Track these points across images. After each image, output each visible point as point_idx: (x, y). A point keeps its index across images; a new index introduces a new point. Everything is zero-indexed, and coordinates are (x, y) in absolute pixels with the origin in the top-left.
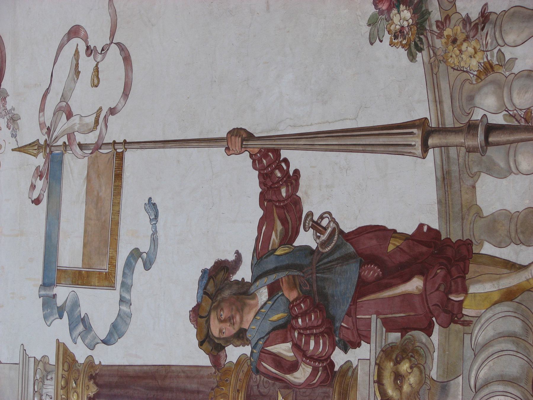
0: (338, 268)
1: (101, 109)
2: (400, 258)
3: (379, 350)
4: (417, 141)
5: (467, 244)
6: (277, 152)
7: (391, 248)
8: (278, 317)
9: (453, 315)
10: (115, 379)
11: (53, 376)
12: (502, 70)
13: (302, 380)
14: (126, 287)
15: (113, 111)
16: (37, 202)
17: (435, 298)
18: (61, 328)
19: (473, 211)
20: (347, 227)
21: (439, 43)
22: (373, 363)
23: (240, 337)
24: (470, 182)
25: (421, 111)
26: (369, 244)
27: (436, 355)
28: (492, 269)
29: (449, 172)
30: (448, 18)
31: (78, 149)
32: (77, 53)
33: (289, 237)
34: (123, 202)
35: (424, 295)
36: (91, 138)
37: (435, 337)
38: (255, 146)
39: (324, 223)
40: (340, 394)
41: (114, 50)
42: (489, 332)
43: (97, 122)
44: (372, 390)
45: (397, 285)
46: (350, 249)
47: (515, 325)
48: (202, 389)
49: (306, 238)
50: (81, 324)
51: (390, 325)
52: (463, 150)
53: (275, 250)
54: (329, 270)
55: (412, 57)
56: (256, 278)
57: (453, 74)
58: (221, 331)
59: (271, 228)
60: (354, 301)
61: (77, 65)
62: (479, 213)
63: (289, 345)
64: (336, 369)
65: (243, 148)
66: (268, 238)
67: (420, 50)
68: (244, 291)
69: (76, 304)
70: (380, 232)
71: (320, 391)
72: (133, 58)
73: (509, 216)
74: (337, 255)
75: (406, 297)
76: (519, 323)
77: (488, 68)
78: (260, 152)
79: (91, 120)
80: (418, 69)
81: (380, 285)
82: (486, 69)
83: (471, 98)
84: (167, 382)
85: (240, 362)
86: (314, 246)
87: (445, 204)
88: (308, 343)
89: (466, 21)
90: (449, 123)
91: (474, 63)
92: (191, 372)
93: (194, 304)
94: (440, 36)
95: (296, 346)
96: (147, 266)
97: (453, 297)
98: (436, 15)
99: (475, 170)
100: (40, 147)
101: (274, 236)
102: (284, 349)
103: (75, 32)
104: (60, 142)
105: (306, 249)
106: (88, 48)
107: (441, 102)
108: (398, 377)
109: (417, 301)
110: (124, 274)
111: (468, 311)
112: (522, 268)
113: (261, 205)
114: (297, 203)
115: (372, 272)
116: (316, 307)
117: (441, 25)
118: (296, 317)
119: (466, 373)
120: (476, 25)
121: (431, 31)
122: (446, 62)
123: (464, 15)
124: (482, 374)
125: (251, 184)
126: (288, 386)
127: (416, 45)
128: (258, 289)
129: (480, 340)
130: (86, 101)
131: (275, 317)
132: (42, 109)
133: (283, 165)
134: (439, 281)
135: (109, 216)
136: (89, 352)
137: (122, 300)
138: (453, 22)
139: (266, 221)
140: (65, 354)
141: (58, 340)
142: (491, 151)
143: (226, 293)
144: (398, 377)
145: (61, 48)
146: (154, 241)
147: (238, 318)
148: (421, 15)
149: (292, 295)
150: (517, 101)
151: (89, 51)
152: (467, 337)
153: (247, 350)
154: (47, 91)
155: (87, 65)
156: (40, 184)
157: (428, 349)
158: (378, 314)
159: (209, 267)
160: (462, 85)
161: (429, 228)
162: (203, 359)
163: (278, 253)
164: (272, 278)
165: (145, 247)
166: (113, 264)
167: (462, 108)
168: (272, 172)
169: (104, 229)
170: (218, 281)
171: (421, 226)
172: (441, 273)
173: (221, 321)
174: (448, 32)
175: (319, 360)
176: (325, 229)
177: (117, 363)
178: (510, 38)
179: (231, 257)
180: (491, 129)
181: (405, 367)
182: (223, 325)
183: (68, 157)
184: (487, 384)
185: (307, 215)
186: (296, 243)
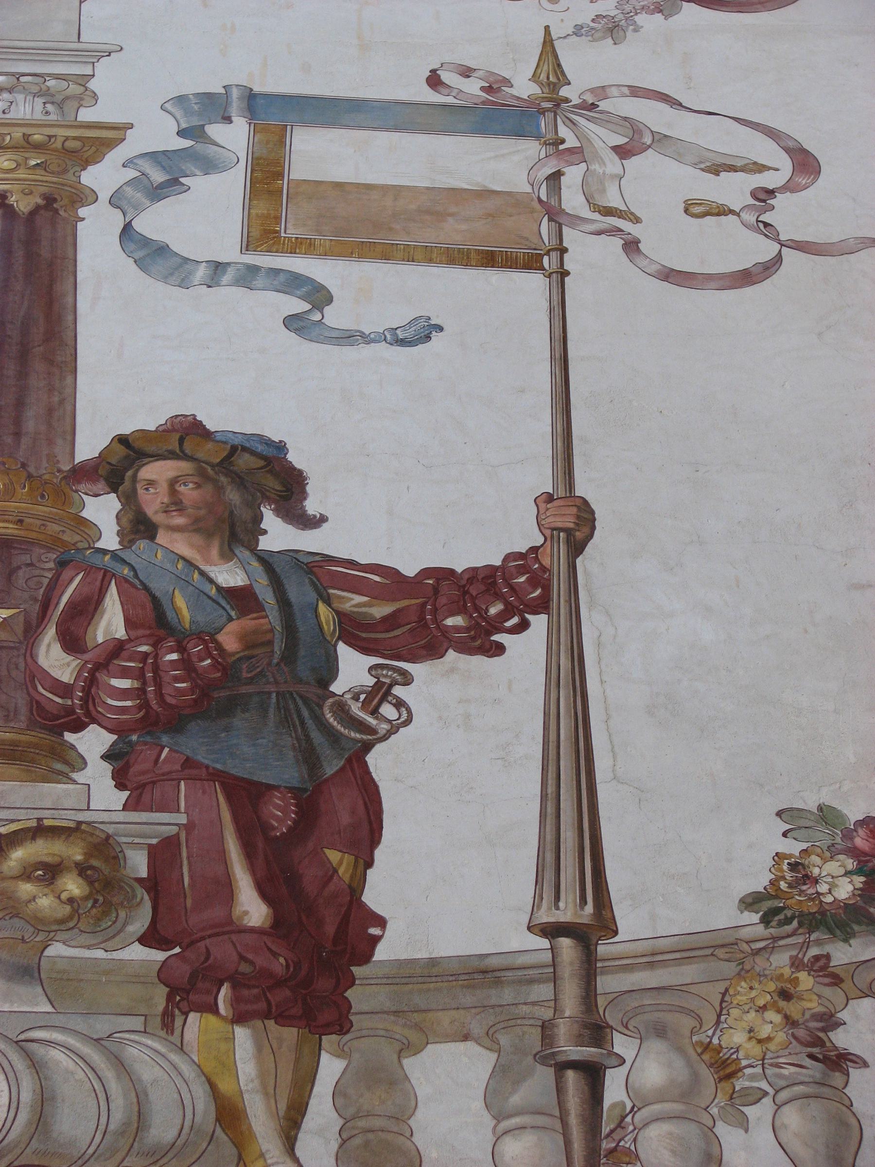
0: (288, 741)
1: (637, 220)
2: (310, 875)
3: (110, 829)
4: (566, 913)
6: (542, 606)
7: (333, 856)
8: (183, 609)
9: (184, 994)
10: (45, 252)
11: (53, 117)
12: (721, 1099)
13: (43, 661)
14: (248, 277)
15: (632, 246)
17: (223, 951)
18: (157, 132)
19: (414, 1036)
20: (378, 761)
21: (781, 960)
22: (81, 817)
23: (138, 526)
24: (477, 1029)
25: (632, 923)
26: (342, 808)
27: (99, 954)
28: (286, 1077)
29: (498, 982)
30: (836, 980)
31: (549, 171)
32: (759, 168)
33: (357, 633)
34: (435, 271)
35: (230, 927)
36: (572, 200)
37: (137, 953)
38: (556, 559)
40: (14, 743)
41: (767, 250)
43: (608, 212)
44: (21, 814)
46: (331, 767)
47: (163, 1129)
48: (25, 441)
49: (353, 669)
50: (167, 176)
51: (163, 853)
52: (548, 1014)
53: (328, 602)
55: (750, 902)
56: (266, 561)
57: (714, 993)
58: (151, 483)
59: (377, 594)
61: (733, 169)
62: (409, 1048)
63: (120, 632)
64: (69, 737)
65: (550, 532)
66: (355, 586)
67: (766, 920)
68: (238, 535)
69: (209, 166)
70: (366, 832)
71: (20, 700)
72: (748, 291)
73: (402, 1116)
74: (317, 737)
75: (225, 890)
76: (169, 1135)
77: (726, 1069)
78: (543, 569)
79: (613, 200)
80: (725, 915)
81: (251, 833)
82: (724, 1063)
83: (661, 1031)
84: (38, 366)
86: (338, 687)
87: (429, 973)
88: (124, 673)
89: (829, 1021)
90: (606, 984)
91: (738, 1038)
92: (61, 419)
93: (211, 426)
94: (796, 964)
95: (117, 648)
96: (293, 322)
97: (224, 992)
98: (842, 954)
99: (504, 1040)
100: (554, 87)
101: (359, 599)
102: (111, 622)
103: (806, 164)
104: (563, 131)
105: (330, 670)
106: (771, 193)
107: (651, 965)
108: (50, 872)
109: (216, 913)
110: (276, 272)
111: (195, 1024)
112: (290, 1143)
113: (427, 572)
114: (432, 650)
115: (279, 814)
116: (204, 691)
117: (821, 966)
118: (180, 648)
121: (807, 945)
123: (843, 1015)
124: (56, 1054)
126: (31, 631)
127: (776, 911)
129: (132, 1052)
130: (654, 187)
131: (181, 602)
132: (636, 92)
133: (515, 620)
134: (261, 961)
135: (402, 239)
136: (104, 196)
137: (218, 267)
138: (827, 992)
140: (100, 142)
141: (131, 126)
142: (545, 1075)
143: (233, 496)
144: (50, 872)
146: (349, 338)
147: (180, 521)
148: (841, 922)
150: (654, 1132)
152: (137, 1023)
153: (110, 541)
155: (734, 190)
156: (473, 87)
157: (109, 938)
158: (189, 827)
159: (290, 457)
160: (688, 1012)
161: (376, 939)
162: (89, 444)
163: (322, 608)
164: (266, 595)
165: (335, 317)
166: (297, 247)
167: (638, 1011)
168: (499, 596)
169: (373, 228)
170: (264, 476)
171: (381, 922)
172: (279, 965)
173: (173, 483)
174: (806, 980)
175: (88, 698)
176: (375, 712)
177: (80, 257)
178: (791, 1117)
179: (312, 506)
180: (593, 1075)
182: (163, 488)
183: (531, 148)
184: (36, 1065)
185: (404, 673)
186: (343, 649)
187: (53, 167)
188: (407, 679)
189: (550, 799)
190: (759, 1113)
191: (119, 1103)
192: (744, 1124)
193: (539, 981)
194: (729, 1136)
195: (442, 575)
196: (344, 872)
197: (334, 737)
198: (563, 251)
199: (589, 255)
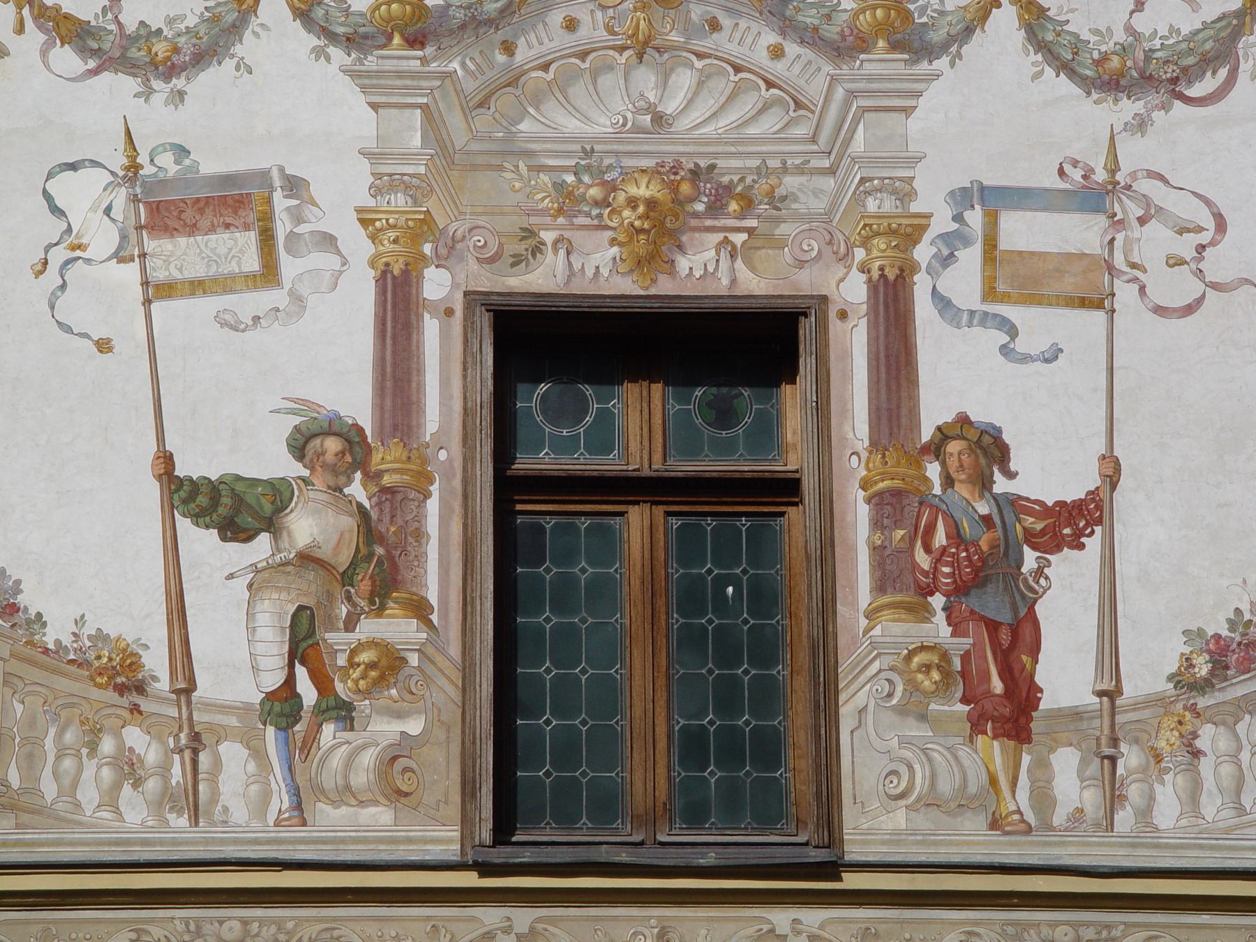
0: (1007, 599)
1: (1145, 271)
3: (946, 647)
4: (1105, 687)
5: (1028, 740)
6: (1099, 522)
7: (1024, 658)
9: (976, 725)
11: (899, 210)
12: (1156, 772)
13: (918, 559)
14: (986, 319)
15: (1142, 289)
16: (1061, 172)
17: (988, 706)
19: (1053, 744)
21: (1180, 706)
22: (937, 641)
23: (948, 482)
24: (1075, 742)
25: (1129, 690)
26: (1027, 631)
27: (946, 708)
28: (1011, 764)
29: (1081, 719)
30: (1198, 715)
32: (1199, 229)
33: (1031, 538)
34: (1060, 311)
35: (989, 693)
36: (1119, 261)
38: (1105, 494)
39: (1042, 581)
40: (910, 603)
42: (966, 763)
43: (1134, 266)
44: (915, 640)
45: (995, 659)
46: (1022, 613)
47: (972, 789)
48: (902, 432)
49: (1030, 558)
51: (966, 658)
52: (1098, 733)
54: (1006, 589)
55: (1170, 678)
56: (995, 498)
57: (1155, 722)
58: (951, 454)
60: (983, 618)
61: (1189, 231)
62: (1052, 750)
63: (944, 543)
64: (929, 599)
65: (1103, 476)
66: (1030, 512)
67: (1175, 687)
68: (985, 483)
73: (1049, 781)
74: (1018, 598)
75: (988, 678)
76: (974, 791)
78: (1101, 500)
79: (1136, 260)
82: (1158, 756)
83: (1137, 741)
84: (904, 383)
85: (927, 479)
86: (1024, 570)
87: (1058, 715)
89: (1195, 735)
90: (1120, 719)
91: (1163, 744)
92: (915, 425)
93: (973, 419)
94: (1185, 708)
95: (944, 550)
96: (1005, 350)
98: (1202, 702)
100: (1113, 172)
102: (940, 538)
105: (1020, 563)
106: (1204, 247)
109: (983, 688)
110: (995, 315)
111: (980, 739)
112: (1014, 793)
113: (1057, 503)
114: (1058, 548)
115: (1005, 637)
116: (976, 571)
117: (1193, 709)
118: (967, 550)
119: (935, 739)
120: (1191, 745)
121: (1189, 698)
122: (1165, 714)
123: (1200, 732)
124: (935, 755)
125: (1074, 492)
127: (1179, 682)
128: (988, 502)
129: (960, 753)
130: (1154, 243)
131: (965, 524)
133: (1089, 530)
134: (1001, 709)
136: (924, 266)
137: (972, 313)
138: (1195, 721)
139: (1046, 511)
143: (983, 461)
144: (927, 668)
145: (1207, 202)
146: (1026, 359)
147: (963, 477)
148: (1203, 686)
149: (984, 545)
150: (1134, 787)
151: (1201, 248)
152: (960, 740)
153: (937, 490)
154: (1166, 182)
156: (1076, 175)
158: (974, 645)
161: (1040, 699)
162: (927, 434)
163: (1018, 525)
165: (1021, 346)
168: (1083, 516)
171: (1041, 691)
172: (1007, 711)
173: (960, 453)
175: (935, 578)
176: (1038, 583)
177: (916, 310)
178: (1180, 779)
179: (1013, 466)
180: (1113, 760)
181: (936, 675)
183: (1101, 220)
184: (930, 760)
185: (1048, 561)
186: (1026, 549)
187: (902, 248)
188: (1049, 564)
189: (1101, 627)
190: (1168, 778)
191: (957, 776)
192: (1163, 783)
193: (1094, 718)
194: (1158, 788)
195: (1061, 504)
196: (1028, 666)
197: (1023, 596)
198: (1113, 295)
199: (1125, 294)
